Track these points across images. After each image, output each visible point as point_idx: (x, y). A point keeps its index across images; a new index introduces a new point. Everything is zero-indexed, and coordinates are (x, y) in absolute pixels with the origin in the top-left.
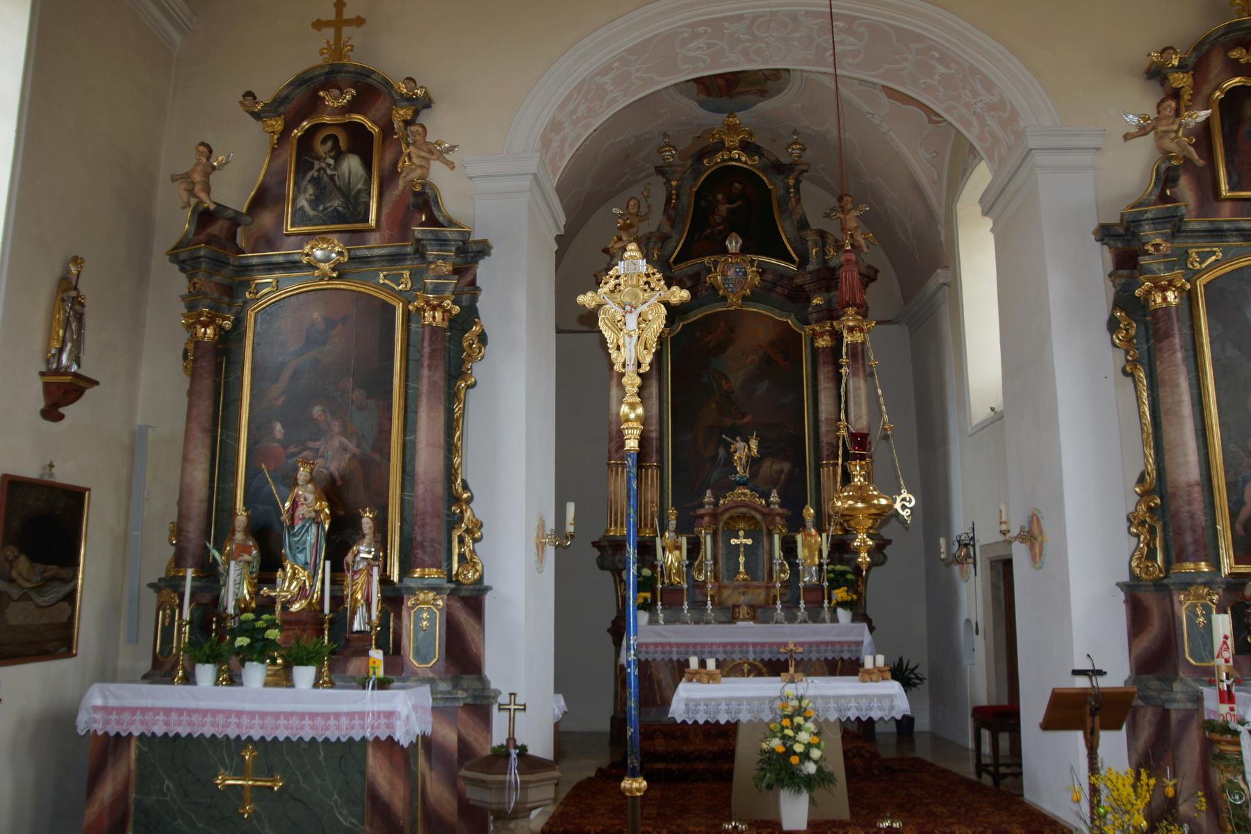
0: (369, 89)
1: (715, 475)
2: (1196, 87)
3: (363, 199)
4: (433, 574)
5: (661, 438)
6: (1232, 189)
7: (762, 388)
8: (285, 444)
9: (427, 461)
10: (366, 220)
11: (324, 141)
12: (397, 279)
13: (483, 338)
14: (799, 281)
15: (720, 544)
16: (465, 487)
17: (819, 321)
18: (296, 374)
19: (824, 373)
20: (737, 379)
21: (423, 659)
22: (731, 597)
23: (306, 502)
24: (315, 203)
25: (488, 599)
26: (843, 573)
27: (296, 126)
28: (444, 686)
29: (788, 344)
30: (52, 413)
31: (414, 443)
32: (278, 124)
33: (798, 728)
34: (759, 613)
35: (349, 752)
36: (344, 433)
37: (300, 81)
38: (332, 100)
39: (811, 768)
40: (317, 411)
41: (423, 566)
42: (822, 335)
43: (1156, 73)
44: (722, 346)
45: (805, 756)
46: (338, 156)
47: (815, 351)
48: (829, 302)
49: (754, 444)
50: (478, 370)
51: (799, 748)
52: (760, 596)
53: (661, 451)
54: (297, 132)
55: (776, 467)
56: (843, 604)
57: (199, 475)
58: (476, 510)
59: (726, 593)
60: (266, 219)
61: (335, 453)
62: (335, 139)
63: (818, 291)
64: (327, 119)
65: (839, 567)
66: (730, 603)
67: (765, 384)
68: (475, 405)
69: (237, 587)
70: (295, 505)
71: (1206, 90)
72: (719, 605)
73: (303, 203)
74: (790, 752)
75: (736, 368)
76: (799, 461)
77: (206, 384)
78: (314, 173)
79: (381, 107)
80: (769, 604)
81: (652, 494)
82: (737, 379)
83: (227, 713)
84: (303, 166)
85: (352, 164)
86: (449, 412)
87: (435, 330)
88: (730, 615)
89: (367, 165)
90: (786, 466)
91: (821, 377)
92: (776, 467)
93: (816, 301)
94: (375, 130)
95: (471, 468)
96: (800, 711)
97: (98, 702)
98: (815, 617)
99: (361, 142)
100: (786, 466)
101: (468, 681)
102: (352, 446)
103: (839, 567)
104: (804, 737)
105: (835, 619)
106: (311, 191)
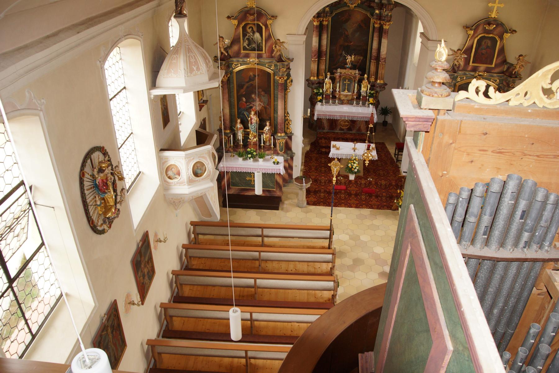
0: (260, 14)
1: (341, 59)
2: (473, 35)
3: (261, 45)
4: (283, 135)
5: (326, 51)
6: (473, 63)
7: (357, 35)
8: (246, 102)
9: (280, 112)
10: (262, 51)
11: (249, 28)
12: (271, 66)
13: (292, 81)
14: (372, 5)
15: (341, 83)
16: (288, 114)
17: (376, 19)
18: (247, 87)
19: (376, 35)
20: (350, 31)
21: (281, 151)
22: (343, 98)
23: (254, 119)
24: (248, 45)
25: (293, 137)
26: (372, 94)
27: (241, 24)
28: (285, 156)
29: (366, 21)
30: (200, 110)
31: (277, 105)
32: (236, 22)
33: (354, 163)
34: (350, 102)
35: (272, 175)
36: (260, 101)
37: (241, 11)
38: (251, 18)
39: (356, 170)
40: (253, 96)
41: (280, 133)
42: (377, 23)
43: (467, 27)
44: (347, 21)
45: (355, 168)
46: (254, 33)
47: (374, 27)
48: (380, 13)
49: (353, 56)
50: (290, 88)
51: (354, 167)
52: (350, 98)
53: (326, 55)
54: (241, 26)
55: (359, 58)
56: (372, 104)
57: (227, 111)
58: (291, 118)
59: (341, 96)
60: (235, 48)
61: (258, 105)
62: (252, 28)
63: (378, 9)
64: (249, 22)
65: (372, 92)
66: (342, 99)
67: (358, 33)
68: (290, 95)
69: (240, 136)
70: (251, 119)
71: (476, 35)
72: (339, 99)
73: (245, 45)
74: (352, 167)
75: (350, 28)
76: (365, 57)
77: (226, 91)
78: (247, 37)
79: (263, 20)
80: (352, 99)
81: (323, 67)
82: (350, 31)
83: (248, 168)
84: (244, 35)
85: (257, 35)
86: (285, 102)
87: (282, 84)
88: (342, 102)
89: (262, 36)
90: (362, 58)
91: (375, 36)
92: (359, 58)
93: (377, 12)
94: (264, 27)
95: (289, 110)
96: (355, 159)
97: (222, 166)
98: (364, 104)
99: (260, 31)
100: (362, 58)
101: (289, 152)
102: (262, 104)
103: (372, 92)
104: (355, 165)
105: (369, 107)
106: (247, 42)
